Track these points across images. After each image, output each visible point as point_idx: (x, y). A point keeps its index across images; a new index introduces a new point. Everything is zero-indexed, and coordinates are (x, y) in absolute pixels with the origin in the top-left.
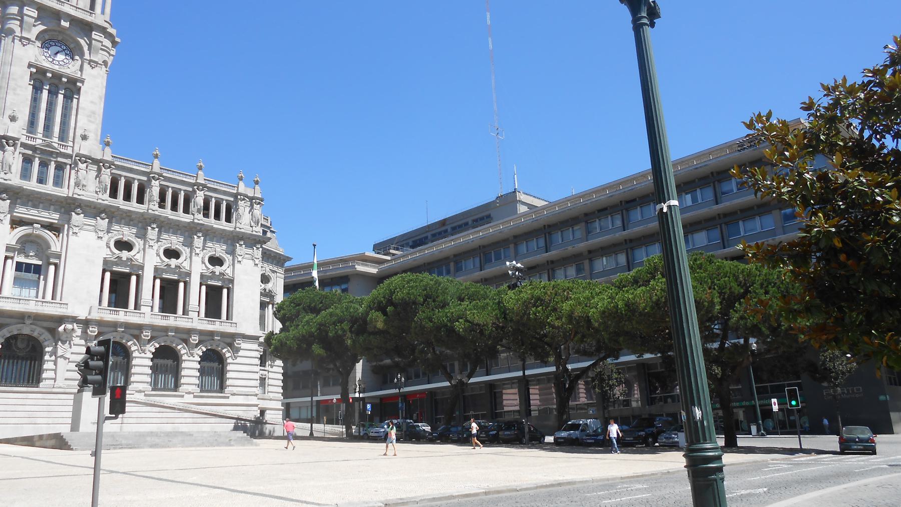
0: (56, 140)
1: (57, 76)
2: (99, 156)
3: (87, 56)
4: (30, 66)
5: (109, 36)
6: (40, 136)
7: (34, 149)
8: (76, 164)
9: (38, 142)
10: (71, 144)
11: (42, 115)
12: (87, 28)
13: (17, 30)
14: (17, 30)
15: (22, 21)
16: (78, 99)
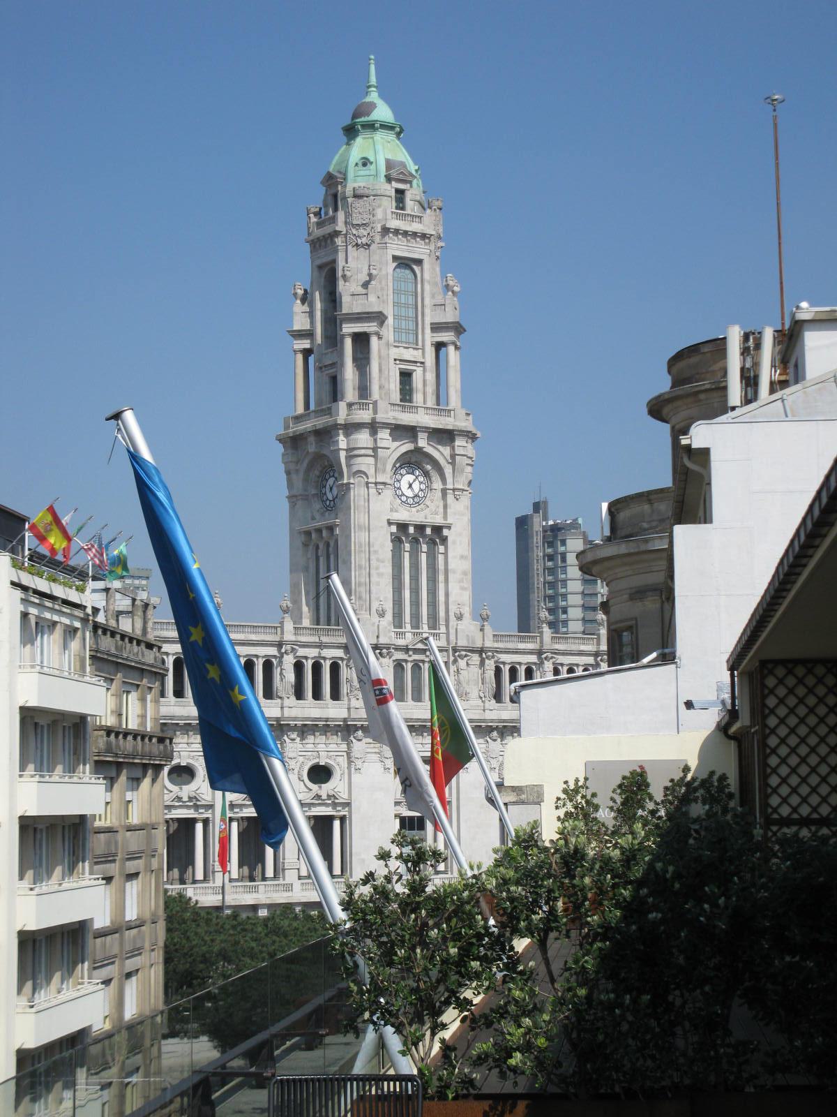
0: (425, 628)
1: (420, 528)
2: (479, 644)
3: (450, 486)
4: (390, 523)
5: (472, 437)
6: (408, 627)
7: (406, 650)
8: (455, 661)
9: (408, 639)
10: (443, 629)
11: (407, 594)
12: (445, 436)
13: (371, 472)
14: (371, 472)
15: (375, 456)
16: (446, 554)
